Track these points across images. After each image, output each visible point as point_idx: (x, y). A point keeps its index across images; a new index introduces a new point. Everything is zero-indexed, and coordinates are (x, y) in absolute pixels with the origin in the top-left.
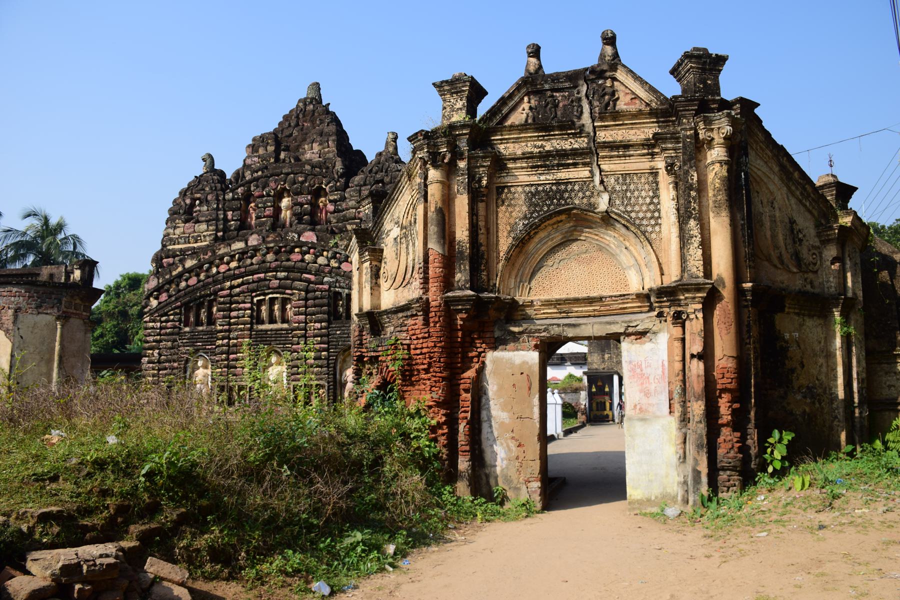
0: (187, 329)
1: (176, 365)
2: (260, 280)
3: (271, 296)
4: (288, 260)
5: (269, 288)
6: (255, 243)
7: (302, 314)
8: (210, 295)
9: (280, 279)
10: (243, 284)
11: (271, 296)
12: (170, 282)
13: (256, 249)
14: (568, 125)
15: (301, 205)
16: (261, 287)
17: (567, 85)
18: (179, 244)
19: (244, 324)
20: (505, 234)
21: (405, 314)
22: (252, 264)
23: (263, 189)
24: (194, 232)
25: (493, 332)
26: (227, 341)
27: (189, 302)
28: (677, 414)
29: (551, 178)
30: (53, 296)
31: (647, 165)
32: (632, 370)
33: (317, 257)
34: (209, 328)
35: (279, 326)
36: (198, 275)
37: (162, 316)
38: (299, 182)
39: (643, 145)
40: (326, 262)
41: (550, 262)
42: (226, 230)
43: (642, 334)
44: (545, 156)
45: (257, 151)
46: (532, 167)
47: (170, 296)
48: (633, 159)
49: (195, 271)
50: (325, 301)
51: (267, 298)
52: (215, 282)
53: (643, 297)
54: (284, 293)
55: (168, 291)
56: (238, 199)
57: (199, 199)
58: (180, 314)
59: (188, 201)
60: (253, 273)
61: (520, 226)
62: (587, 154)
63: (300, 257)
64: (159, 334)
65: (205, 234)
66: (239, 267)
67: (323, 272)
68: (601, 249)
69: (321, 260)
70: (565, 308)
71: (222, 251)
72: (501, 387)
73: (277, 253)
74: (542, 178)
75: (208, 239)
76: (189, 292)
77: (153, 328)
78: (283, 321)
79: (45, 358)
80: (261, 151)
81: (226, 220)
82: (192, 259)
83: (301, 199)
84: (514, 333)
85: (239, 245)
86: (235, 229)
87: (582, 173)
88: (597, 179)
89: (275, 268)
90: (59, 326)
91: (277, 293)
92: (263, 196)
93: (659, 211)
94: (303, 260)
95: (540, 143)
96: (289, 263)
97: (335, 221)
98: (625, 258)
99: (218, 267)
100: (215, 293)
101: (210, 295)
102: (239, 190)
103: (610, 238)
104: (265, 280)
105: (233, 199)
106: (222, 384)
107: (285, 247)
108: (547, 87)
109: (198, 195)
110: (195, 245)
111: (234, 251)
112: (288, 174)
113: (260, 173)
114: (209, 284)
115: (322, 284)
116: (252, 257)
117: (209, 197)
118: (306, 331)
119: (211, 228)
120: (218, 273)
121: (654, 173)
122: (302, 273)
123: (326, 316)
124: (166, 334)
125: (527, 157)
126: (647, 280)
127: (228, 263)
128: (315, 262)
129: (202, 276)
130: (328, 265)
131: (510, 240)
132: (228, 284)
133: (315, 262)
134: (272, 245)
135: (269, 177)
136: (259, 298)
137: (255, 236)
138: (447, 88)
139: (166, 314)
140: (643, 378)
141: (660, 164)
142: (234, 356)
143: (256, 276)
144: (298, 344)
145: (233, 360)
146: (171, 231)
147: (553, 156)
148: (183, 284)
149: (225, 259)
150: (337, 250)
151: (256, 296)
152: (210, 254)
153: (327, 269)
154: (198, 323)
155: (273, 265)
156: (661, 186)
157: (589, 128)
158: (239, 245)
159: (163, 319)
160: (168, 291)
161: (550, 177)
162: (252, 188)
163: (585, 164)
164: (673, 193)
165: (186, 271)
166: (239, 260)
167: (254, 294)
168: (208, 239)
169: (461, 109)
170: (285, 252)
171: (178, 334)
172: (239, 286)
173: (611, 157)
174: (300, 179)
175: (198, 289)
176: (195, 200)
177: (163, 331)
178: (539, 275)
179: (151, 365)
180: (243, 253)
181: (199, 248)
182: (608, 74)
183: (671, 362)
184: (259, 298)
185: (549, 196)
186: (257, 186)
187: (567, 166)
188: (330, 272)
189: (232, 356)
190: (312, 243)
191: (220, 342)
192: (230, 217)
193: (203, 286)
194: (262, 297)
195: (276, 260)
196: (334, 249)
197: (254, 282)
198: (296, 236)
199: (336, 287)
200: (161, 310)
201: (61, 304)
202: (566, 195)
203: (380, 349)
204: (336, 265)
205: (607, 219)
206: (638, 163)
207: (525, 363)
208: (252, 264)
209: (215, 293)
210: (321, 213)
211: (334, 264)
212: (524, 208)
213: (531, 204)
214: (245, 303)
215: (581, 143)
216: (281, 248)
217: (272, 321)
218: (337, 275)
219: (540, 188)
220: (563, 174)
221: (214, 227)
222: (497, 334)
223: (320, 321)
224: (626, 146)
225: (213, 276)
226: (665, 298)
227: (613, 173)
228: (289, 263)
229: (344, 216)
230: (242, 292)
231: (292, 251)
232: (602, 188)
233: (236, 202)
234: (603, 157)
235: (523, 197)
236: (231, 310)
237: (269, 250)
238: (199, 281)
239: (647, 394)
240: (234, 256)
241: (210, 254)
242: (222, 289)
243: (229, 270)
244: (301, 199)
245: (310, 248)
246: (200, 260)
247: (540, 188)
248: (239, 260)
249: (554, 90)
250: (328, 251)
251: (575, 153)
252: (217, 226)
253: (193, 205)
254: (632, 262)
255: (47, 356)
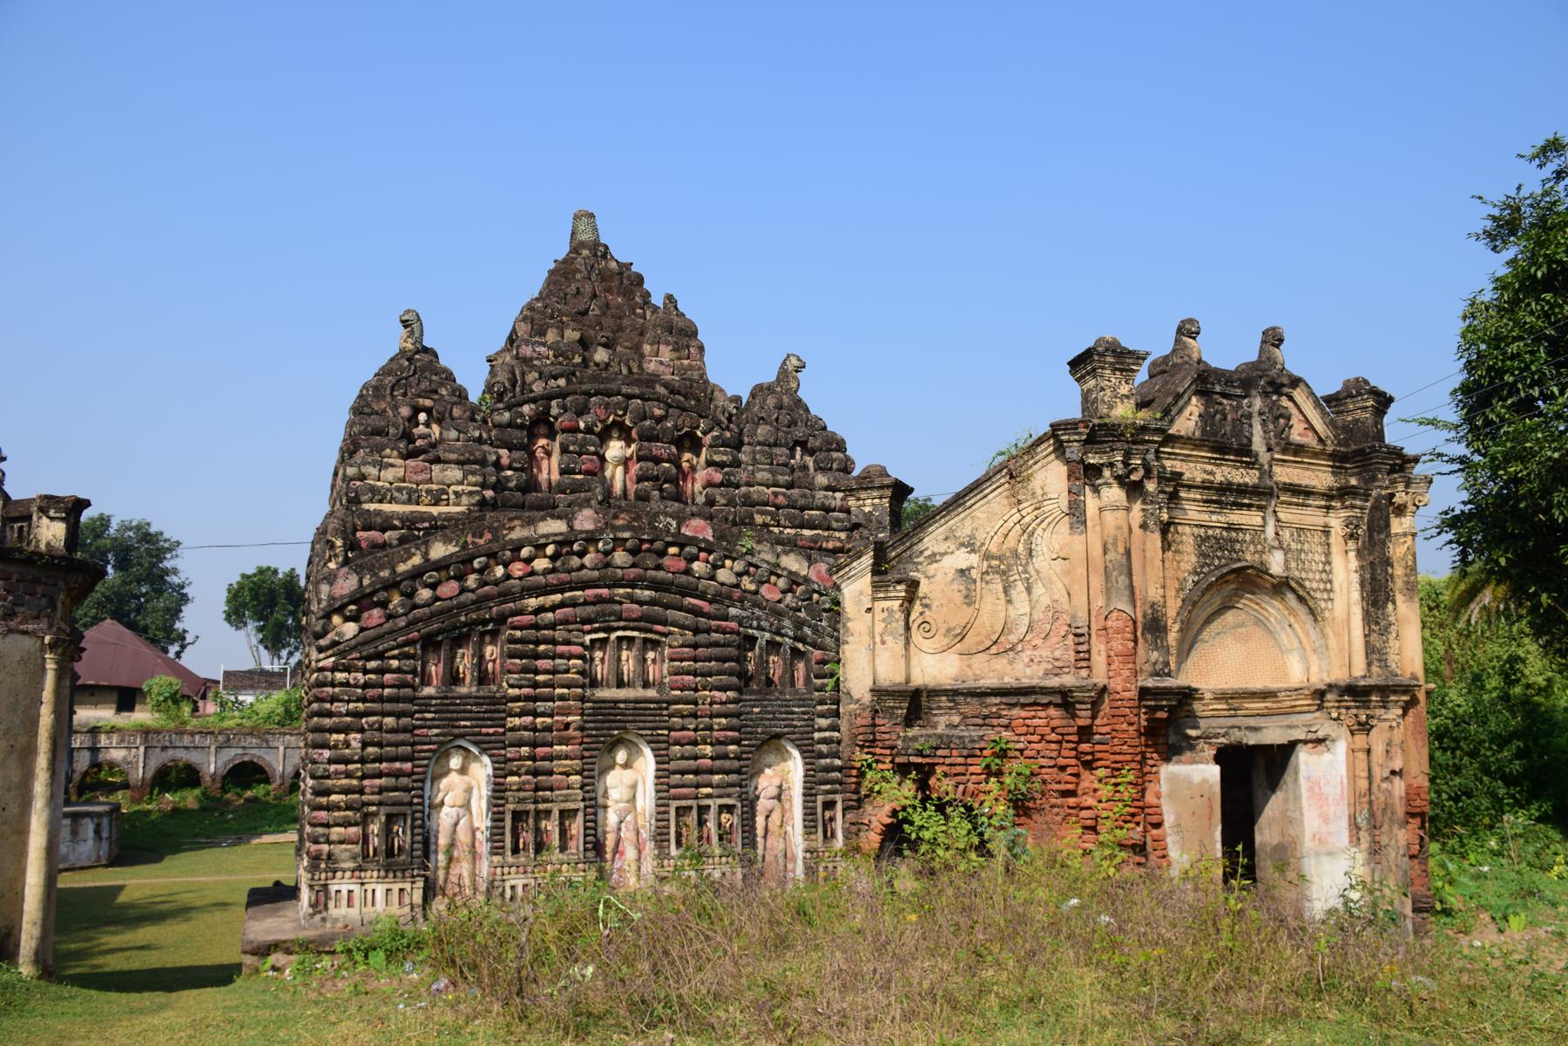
0: (429, 691)
1: (408, 766)
2: (599, 600)
3: (620, 633)
4: (659, 567)
5: (620, 619)
6: (589, 526)
7: (688, 673)
8: (485, 622)
9: (641, 603)
10: (562, 605)
11: (620, 633)
12: (392, 585)
13: (591, 539)
14: (1244, 453)
15: (657, 461)
16: (603, 617)
17: (1239, 392)
18: (392, 500)
19: (568, 687)
20: (1173, 593)
21: (1004, 700)
22: (583, 567)
23: (580, 414)
24: (430, 481)
25: (1166, 736)
26: (530, 718)
27: (439, 632)
28: (1365, 845)
29: (1222, 519)
30: (40, 589)
31: (1321, 521)
32: (1311, 789)
33: (715, 567)
34: (484, 692)
35: (639, 693)
36: (460, 577)
37: (369, 658)
38: (653, 417)
39: (1324, 495)
40: (733, 580)
41: (1205, 635)
42: (499, 486)
43: (1320, 741)
44: (1226, 488)
45: (543, 334)
46: (1206, 501)
47: (389, 617)
48: (1309, 511)
49: (459, 567)
50: (732, 651)
51: (613, 636)
52: (506, 596)
53: (1320, 694)
54: (651, 631)
55: (383, 604)
56: (521, 427)
57: (428, 411)
58: (412, 657)
59: (405, 411)
60: (584, 585)
61: (1190, 585)
62: (1263, 494)
63: (682, 564)
64: (363, 700)
65: (459, 488)
66: (553, 570)
67: (729, 597)
68: (1260, 623)
69: (724, 575)
70: (1235, 703)
71: (518, 534)
72: (1178, 816)
73: (633, 552)
74: (1214, 518)
75: (465, 500)
76: (441, 612)
77: (347, 684)
78: (646, 685)
79: (18, 746)
80: (551, 336)
81: (497, 465)
82: (447, 541)
83: (659, 449)
84: (1190, 737)
85: (556, 526)
86: (518, 488)
87: (1251, 518)
88: (1270, 530)
89: (634, 580)
90: (51, 666)
91: (633, 629)
92: (576, 430)
93: (1330, 581)
94: (688, 572)
95: (1209, 468)
96: (661, 574)
97: (723, 501)
98: (1285, 638)
99: (506, 565)
100: (501, 619)
101: (485, 622)
102: (526, 409)
103: (1273, 609)
104: (611, 601)
105: (510, 425)
106: (521, 807)
107: (651, 542)
108: (1218, 388)
109: (428, 403)
110: (435, 511)
111: (545, 536)
112: (629, 397)
113: (562, 382)
114: (488, 598)
115: (726, 618)
116: (581, 554)
117: (456, 412)
118: (696, 704)
119: (471, 478)
120: (508, 577)
121: (1326, 532)
122: (684, 595)
123: (735, 680)
124: (381, 699)
125: (1205, 486)
126: (1314, 669)
127: (528, 561)
128: (713, 578)
129: (472, 580)
130: (737, 586)
131: (1179, 602)
132: (533, 602)
133: (713, 578)
134: (626, 535)
135: (591, 396)
136: (594, 636)
137: (587, 512)
138: (1109, 359)
139: (380, 656)
140: (1322, 799)
141: (1336, 521)
142: (547, 749)
143: (590, 592)
144: (683, 728)
145: (543, 759)
146: (373, 471)
147: (1231, 491)
148: (425, 594)
149: (525, 552)
150: (754, 560)
151: (589, 632)
152: (488, 536)
153: (737, 593)
154: (454, 678)
155: (633, 572)
156: (1334, 549)
157: (1264, 457)
158: (556, 526)
159: (372, 664)
160: (383, 604)
161: (1222, 519)
162: (555, 411)
163: (1260, 508)
164: (1354, 563)
165: (430, 566)
166: (553, 558)
167: (587, 627)
168: (465, 500)
169: (1127, 397)
170: (648, 550)
171: (412, 700)
172: (553, 608)
173: (1291, 504)
174: (658, 412)
175: (461, 607)
176: (417, 410)
177: (371, 692)
178: (1193, 653)
179: (342, 767)
180: (564, 543)
181: (449, 517)
182: (1286, 390)
183: (1353, 777)
184: (594, 636)
185: (1220, 544)
186: (565, 409)
187: (1241, 506)
188: (741, 600)
189: (541, 751)
190: (705, 540)
191: (517, 721)
192: (505, 461)
193: (474, 602)
194: (602, 635)
195: (634, 565)
196: (749, 558)
197: (586, 603)
198: (674, 523)
199: (751, 627)
200: (369, 648)
201: (54, 608)
202: (1238, 546)
203: (939, 753)
204: (753, 587)
205: (1282, 587)
206: (1311, 516)
207: (1205, 781)
208: (583, 567)
209: (501, 619)
210: (685, 480)
211: (747, 584)
212: (1194, 559)
213: (1204, 555)
214: (568, 643)
215: (1250, 477)
216: (642, 541)
217: (620, 684)
218: (756, 605)
219: (1210, 532)
220: (1236, 517)
221: (479, 479)
222: (1172, 739)
223: (723, 689)
224: (1307, 492)
225: (496, 583)
226: (1358, 697)
227: (1289, 525)
228: (661, 574)
229: (747, 496)
230: (565, 622)
231: (662, 553)
232: (1276, 544)
233: (518, 433)
234: (1283, 503)
235: (1191, 540)
236: (537, 656)
237: (619, 542)
238: (463, 590)
239: (1326, 820)
240: (546, 545)
241: (488, 536)
242: (520, 612)
243: (533, 573)
244: (659, 449)
245: (701, 550)
246: (464, 547)
247: (1210, 532)
248: (553, 558)
249: (1224, 395)
250: (734, 560)
251: (1242, 490)
252: (484, 475)
253: (413, 420)
254: (1296, 644)
255: (23, 740)
